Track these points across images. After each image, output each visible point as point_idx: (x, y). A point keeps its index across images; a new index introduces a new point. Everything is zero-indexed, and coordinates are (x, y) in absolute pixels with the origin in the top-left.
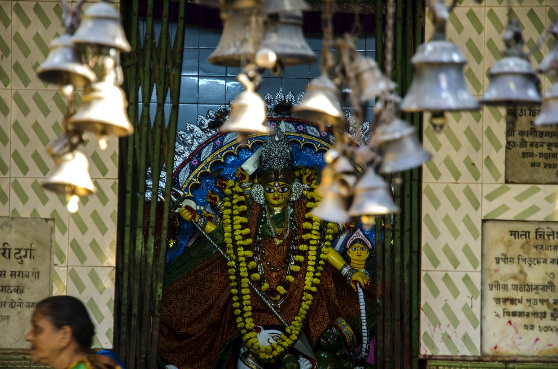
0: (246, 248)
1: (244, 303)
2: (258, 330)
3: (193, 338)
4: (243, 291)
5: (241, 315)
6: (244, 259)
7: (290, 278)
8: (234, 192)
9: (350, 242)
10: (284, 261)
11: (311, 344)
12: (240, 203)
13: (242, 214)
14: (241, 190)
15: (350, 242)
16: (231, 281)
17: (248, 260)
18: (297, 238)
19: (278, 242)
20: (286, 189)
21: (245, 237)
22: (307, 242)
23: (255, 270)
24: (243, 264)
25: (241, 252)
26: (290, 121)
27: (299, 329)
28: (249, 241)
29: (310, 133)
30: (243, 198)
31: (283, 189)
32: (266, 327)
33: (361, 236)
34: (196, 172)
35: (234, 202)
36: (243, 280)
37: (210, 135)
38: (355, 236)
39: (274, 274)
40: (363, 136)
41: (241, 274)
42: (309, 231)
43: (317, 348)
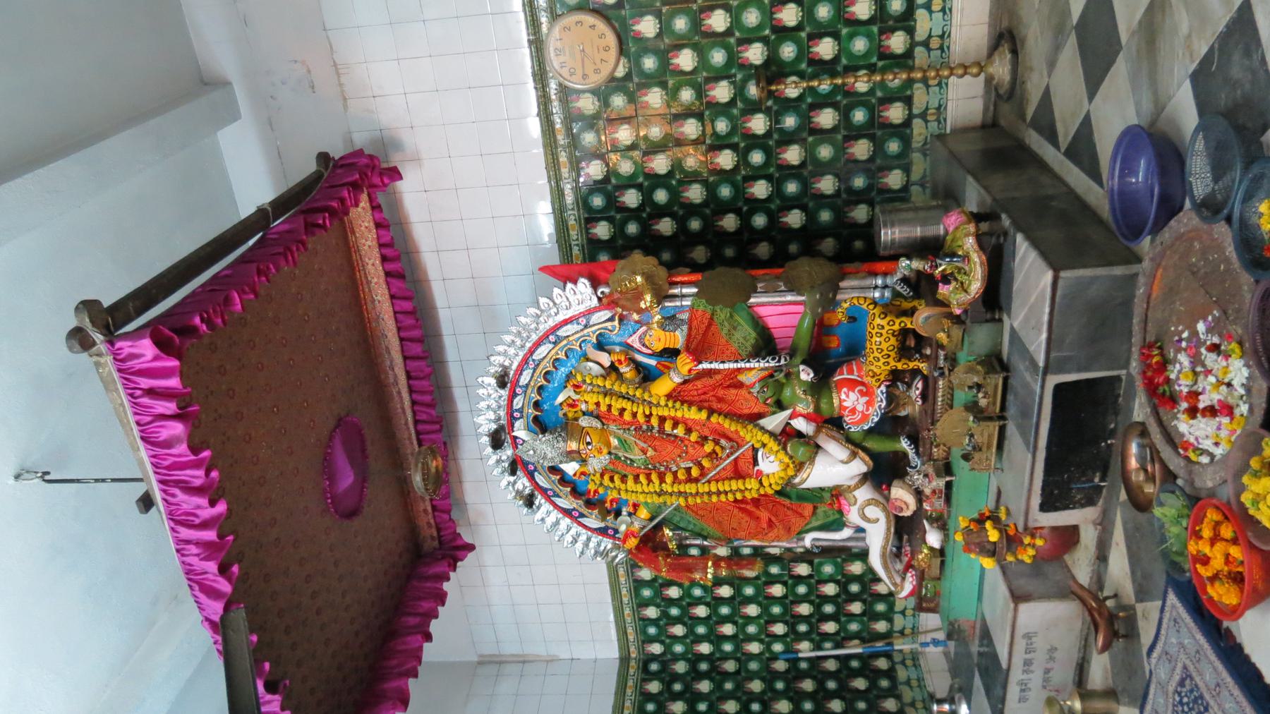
0: (662, 480)
1: (728, 489)
2: (760, 473)
3: (773, 519)
5: (742, 491)
8: (601, 484)
9: (644, 350)
10: (673, 442)
11: (774, 413)
12: (612, 479)
13: (624, 479)
14: (598, 475)
15: (644, 350)
17: (675, 479)
18: (645, 427)
19: (650, 453)
21: (650, 481)
22: (649, 417)
23: (688, 470)
25: (667, 487)
27: (755, 431)
28: (654, 477)
30: (606, 477)
31: (588, 444)
32: (755, 462)
38: (637, 345)
39: (691, 450)
40: (512, 351)
41: (694, 491)
42: (634, 415)
43: (780, 406)
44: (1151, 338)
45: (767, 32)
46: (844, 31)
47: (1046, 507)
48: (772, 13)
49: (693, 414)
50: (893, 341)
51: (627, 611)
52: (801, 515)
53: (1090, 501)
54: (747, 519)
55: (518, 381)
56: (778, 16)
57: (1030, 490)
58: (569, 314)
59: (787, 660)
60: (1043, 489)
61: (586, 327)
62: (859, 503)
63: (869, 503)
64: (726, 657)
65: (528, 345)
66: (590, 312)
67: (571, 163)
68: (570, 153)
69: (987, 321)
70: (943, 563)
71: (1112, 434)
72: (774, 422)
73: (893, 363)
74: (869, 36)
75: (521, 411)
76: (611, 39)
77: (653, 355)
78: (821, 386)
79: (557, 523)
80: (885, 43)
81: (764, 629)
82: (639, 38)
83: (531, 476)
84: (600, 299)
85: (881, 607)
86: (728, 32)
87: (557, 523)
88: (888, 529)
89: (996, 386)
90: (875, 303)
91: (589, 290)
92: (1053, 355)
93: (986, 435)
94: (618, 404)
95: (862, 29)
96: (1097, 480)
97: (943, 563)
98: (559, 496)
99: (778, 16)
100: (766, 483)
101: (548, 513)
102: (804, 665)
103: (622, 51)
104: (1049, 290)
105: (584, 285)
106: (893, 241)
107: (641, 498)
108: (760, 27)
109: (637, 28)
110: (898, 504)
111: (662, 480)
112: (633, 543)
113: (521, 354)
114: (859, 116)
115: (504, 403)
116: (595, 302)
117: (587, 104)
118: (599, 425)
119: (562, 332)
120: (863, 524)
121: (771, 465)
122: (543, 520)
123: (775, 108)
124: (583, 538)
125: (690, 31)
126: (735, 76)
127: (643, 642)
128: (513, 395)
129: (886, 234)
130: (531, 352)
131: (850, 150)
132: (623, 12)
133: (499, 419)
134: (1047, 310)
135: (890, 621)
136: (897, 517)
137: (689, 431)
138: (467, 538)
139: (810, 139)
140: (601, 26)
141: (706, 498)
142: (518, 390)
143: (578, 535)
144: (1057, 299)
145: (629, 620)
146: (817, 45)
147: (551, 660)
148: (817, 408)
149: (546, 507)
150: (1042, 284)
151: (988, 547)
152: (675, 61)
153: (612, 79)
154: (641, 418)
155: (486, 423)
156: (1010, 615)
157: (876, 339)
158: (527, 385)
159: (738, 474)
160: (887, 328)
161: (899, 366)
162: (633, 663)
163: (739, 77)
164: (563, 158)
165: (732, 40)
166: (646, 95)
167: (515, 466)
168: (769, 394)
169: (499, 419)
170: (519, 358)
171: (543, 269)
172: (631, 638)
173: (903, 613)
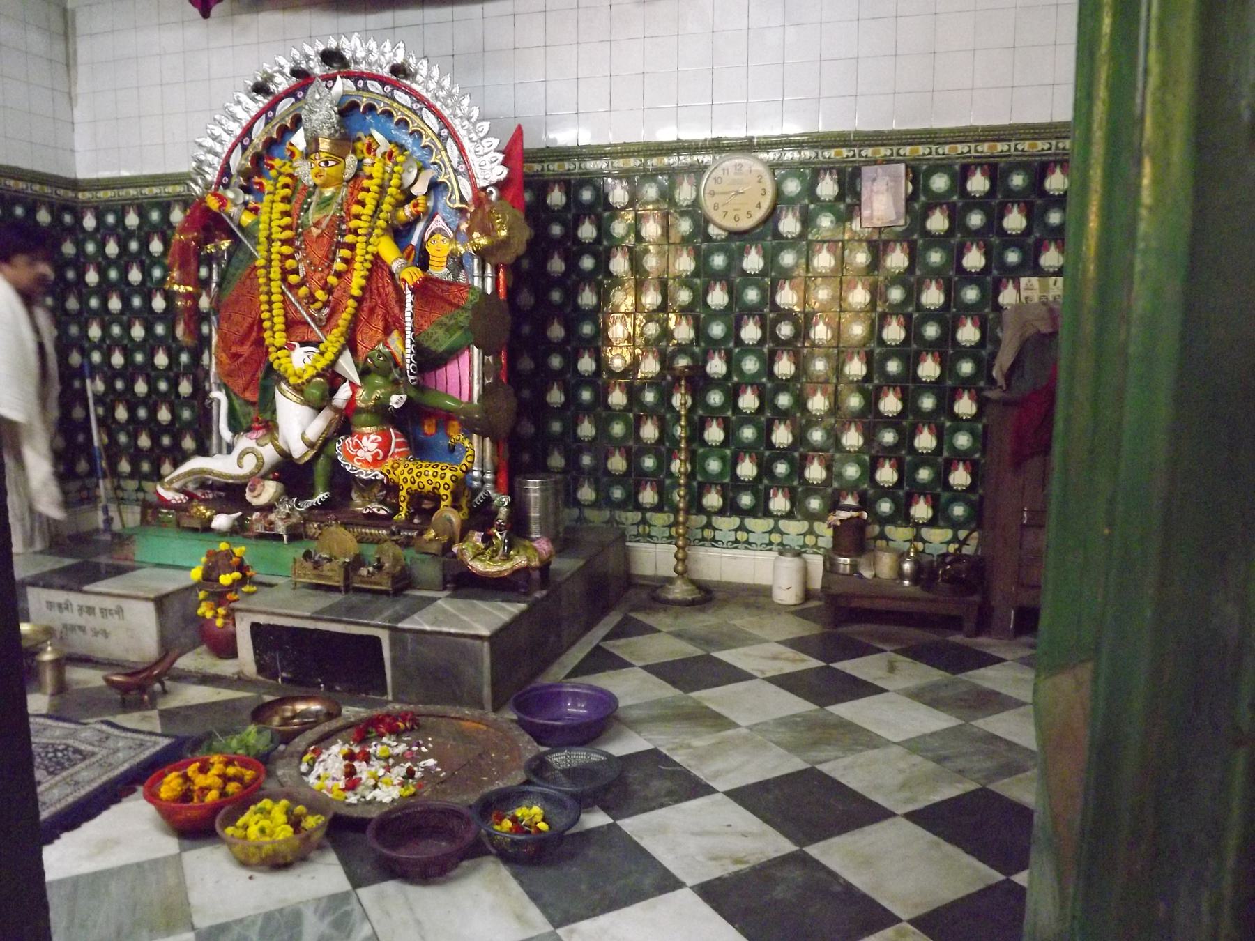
0: (284, 242)
1: (275, 312)
2: (292, 348)
3: (241, 360)
4: (274, 298)
6: (279, 257)
7: (332, 280)
8: (280, 174)
10: (327, 257)
11: (357, 366)
12: (286, 186)
13: (286, 199)
14: (290, 171)
16: (260, 285)
17: (285, 257)
18: (344, 227)
20: (331, 163)
21: (284, 228)
23: (296, 272)
24: (276, 263)
25: (276, 247)
26: (348, 76)
27: (338, 345)
29: (370, 88)
30: (288, 180)
31: (326, 163)
33: (442, 225)
34: (247, 153)
35: (279, 185)
36: (272, 283)
37: (261, 105)
40: (432, 85)
41: (272, 276)
42: (358, 217)
43: (364, 373)
44: (422, 720)
45: (735, 379)
46: (728, 452)
47: (256, 629)
48: (752, 385)
49: (357, 282)
50: (428, 488)
51: (132, 192)
52: (245, 389)
53: (261, 669)
54: (241, 331)
55: (399, 89)
56: (749, 391)
57: (273, 614)
58: (471, 155)
59: (82, 366)
60: (274, 626)
61: (455, 171)
62: (260, 449)
63: (260, 459)
64: (83, 301)
65: (438, 105)
66: (472, 179)
67: (628, 170)
68: (638, 171)
69: (444, 576)
70: (195, 530)
71: (330, 689)
72: (347, 365)
73: (406, 487)
74: (721, 474)
75: (365, 88)
76: (745, 224)
77: (422, 242)
78: (383, 415)
79: (235, 119)
80: (713, 490)
81: (117, 343)
82: (743, 252)
83: (290, 93)
84: (484, 189)
85: (145, 467)
86: (739, 342)
87: (235, 119)
88: (231, 477)
89: (380, 584)
90: (468, 471)
91: (495, 179)
92: (408, 635)
93: (330, 574)
94: (370, 199)
95: (728, 469)
96: (284, 675)
97: (195, 530)
98: (266, 124)
99: (749, 391)
100: (280, 353)
101: (247, 110)
102: (77, 384)
103: (733, 234)
104: (472, 632)
105: (500, 173)
106: (527, 490)
107: (264, 218)
108: (741, 372)
109: (753, 251)
110: (259, 487)
111: (284, 242)
112: (213, 204)
113: (429, 96)
114: (649, 462)
115: (375, 70)
116: (481, 183)
117: (685, 194)
118: (347, 177)
119: (450, 143)
120: (236, 452)
121: (300, 361)
122: (239, 103)
123: (664, 383)
124: (218, 148)
125: (744, 303)
126: (698, 345)
127: (96, 208)
128: (383, 81)
129: (535, 484)
130: (431, 108)
131: (617, 454)
132: (769, 238)
133: (356, 62)
134: (453, 630)
135: (132, 476)
136: (246, 485)
137: (339, 275)
138: (216, 10)
139: (631, 415)
140: (759, 215)
141: (264, 289)
142: (388, 88)
143: (221, 142)
144: (463, 640)
145: (123, 193)
146: (719, 425)
147: (71, 99)
148: (361, 411)
149: (255, 108)
150: (476, 625)
151: (214, 575)
152: (718, 287)
153: (708, 221)
154: (354, 224)
155: (352, 47)
156: (141, 594)
157: (431, 470)
158: (394, 99)
159: (291, 325)
160: (442, 483)
161: (403, 493)
162: (71, 194)
163: (697, 350)
164: (633, 162)
165: (731, 345)
166: (689, 255)
167: (302, 76)
168: (377, 363)
169: (356, 62)
170: (423, 93)
171: (519, 127)
172: (101, 194)
173: (140, 489)
